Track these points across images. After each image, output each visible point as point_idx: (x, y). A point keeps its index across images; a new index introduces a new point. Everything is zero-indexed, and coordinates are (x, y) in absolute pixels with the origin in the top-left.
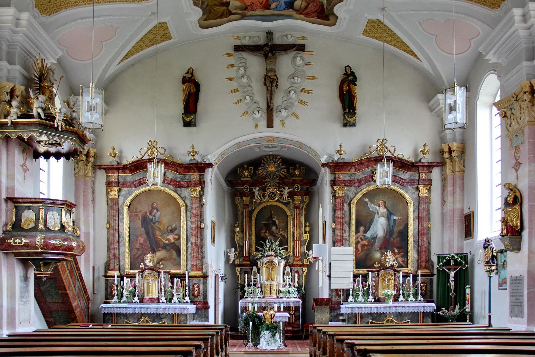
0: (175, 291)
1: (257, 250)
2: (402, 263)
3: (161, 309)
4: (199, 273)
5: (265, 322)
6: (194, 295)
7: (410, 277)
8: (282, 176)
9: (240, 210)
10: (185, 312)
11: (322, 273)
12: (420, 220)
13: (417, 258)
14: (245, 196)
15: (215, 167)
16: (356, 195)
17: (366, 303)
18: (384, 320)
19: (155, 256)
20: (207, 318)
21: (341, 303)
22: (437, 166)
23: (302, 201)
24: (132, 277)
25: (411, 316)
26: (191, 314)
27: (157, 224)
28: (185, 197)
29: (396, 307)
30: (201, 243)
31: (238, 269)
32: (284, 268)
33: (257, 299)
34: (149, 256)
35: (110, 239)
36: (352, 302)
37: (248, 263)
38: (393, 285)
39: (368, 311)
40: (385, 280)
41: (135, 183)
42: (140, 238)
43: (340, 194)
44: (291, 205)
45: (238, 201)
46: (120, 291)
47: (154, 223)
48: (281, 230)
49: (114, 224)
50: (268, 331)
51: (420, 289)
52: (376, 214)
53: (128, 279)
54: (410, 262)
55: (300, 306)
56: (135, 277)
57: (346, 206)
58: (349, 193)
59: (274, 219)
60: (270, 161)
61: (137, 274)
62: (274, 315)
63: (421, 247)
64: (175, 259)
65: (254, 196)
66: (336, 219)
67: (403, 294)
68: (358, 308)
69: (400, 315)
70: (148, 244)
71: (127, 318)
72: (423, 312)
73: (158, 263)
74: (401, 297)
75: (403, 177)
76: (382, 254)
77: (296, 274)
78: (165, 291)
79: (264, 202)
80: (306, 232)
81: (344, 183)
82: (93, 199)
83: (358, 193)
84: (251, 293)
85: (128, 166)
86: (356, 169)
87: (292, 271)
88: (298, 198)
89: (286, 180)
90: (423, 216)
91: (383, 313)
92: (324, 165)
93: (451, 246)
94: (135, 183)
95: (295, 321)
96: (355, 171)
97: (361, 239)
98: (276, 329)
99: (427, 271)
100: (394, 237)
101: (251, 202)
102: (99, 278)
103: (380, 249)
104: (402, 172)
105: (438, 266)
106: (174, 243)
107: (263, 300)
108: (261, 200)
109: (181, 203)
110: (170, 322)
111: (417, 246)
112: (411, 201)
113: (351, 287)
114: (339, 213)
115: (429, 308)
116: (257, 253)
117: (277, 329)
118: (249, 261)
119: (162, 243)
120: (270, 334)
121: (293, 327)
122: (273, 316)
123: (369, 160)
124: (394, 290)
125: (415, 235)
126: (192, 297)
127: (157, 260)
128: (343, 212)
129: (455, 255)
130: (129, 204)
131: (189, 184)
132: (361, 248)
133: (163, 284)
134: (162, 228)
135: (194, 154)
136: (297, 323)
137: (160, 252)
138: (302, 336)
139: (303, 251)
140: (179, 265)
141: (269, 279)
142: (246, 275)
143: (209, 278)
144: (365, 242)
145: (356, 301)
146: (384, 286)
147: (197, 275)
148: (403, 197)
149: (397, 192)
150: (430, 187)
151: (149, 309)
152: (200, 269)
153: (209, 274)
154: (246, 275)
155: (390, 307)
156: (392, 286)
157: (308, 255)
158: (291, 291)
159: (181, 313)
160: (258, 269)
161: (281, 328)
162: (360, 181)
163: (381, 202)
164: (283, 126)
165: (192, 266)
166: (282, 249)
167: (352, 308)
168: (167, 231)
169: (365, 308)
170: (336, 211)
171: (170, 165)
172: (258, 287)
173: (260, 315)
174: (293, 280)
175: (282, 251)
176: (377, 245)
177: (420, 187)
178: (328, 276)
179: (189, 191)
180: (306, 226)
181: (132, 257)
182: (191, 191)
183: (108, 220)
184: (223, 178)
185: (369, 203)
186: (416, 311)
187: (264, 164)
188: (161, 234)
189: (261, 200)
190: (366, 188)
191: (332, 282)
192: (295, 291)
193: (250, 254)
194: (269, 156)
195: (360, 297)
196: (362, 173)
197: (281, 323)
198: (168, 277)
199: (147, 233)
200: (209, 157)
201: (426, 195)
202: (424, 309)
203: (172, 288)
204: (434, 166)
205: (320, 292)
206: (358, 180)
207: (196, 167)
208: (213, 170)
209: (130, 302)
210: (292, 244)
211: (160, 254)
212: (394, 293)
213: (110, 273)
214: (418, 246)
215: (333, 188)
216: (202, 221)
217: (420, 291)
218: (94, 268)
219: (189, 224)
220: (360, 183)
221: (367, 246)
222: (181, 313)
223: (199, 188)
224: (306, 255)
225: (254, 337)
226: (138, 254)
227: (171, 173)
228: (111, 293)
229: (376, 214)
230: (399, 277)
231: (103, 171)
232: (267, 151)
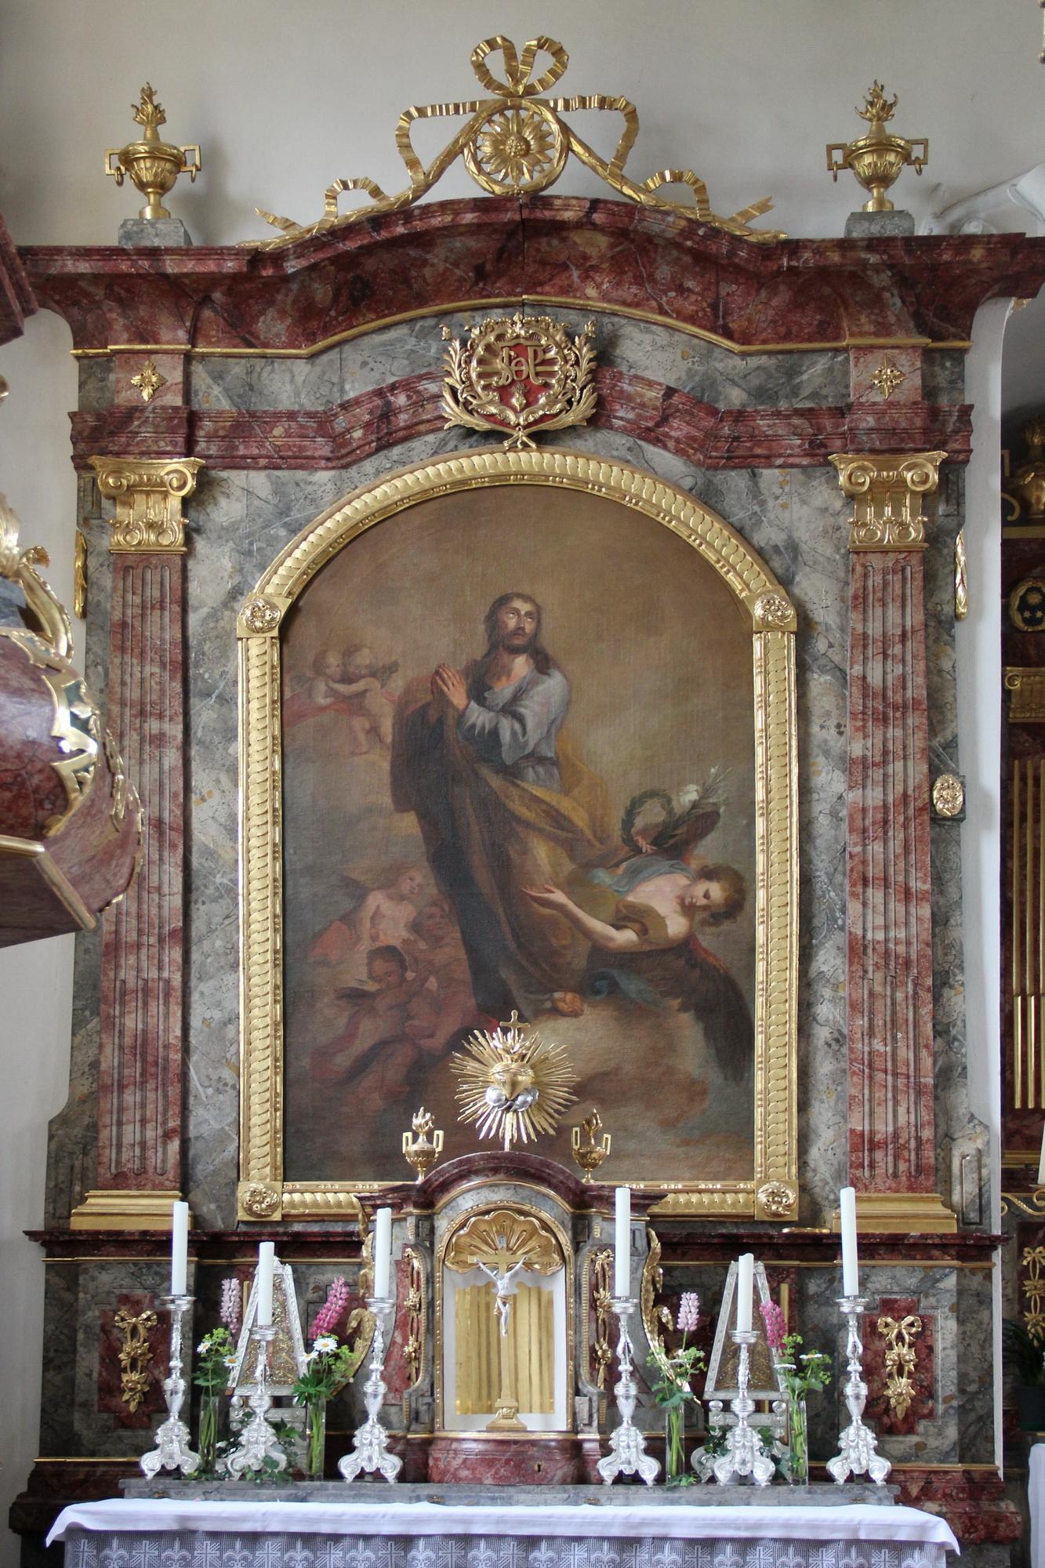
27: (535, 783)
42: (376, 900)
47: (511, 773)
64: (695, 1090)
70: (452, 951)
106: (686, 947)
119: (584, 947)
134: (580, 819)
137: (563, 1024)
165: (856, 1148)
168: (629, 840)
188: (568, 867)
227: (662, 337)
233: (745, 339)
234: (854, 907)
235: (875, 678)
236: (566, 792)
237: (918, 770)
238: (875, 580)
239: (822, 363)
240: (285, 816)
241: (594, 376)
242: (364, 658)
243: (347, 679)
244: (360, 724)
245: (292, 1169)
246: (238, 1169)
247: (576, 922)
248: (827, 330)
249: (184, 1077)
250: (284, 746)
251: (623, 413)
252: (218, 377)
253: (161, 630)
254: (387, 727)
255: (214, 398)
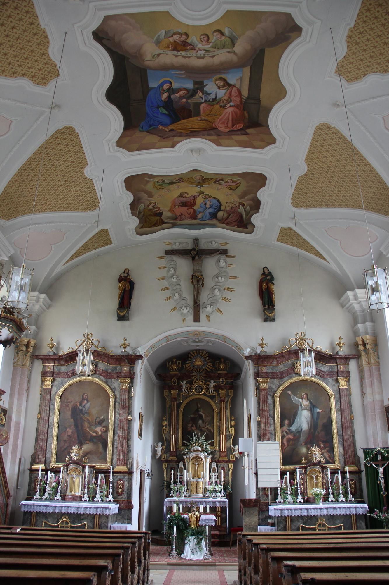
0: (98, 488)
1: (184, 445)
2: (328, 458)
3: (82, 509)
4: (124, 469)
5: (190, 525)
6: (117, 492)
7: (338, 473)
8: (208, 370)
9: (168, 403)
10: (107, 512)
11: (249, 470)
12: (343, 412)
13: (343, 453)
14: (173, 389)
15: (145, 360)
16: (279, 387)
17: (295, 504)
18: (315, 525)
19: (81, 449)
20: (129, 521)
21: (270, 504)
22: (354, 358)
23: (227, 395)
24: (57, 471)
25: (343, 519)
26: (113, 515)
27: (86, 416)
28: (115, 388)
29: (327, 508)
30: (127, 436)
31: (165, 465)
32: (211, 464)
33: (183, 498)
34: (75, 448)
35: (40, 430)
36: (280, 502)
37: (175, 458)
38: (321, 483)
39: (298, 513)
40: (313, 478)
41: (68, 373)
42: (68, 429)
43: (264, 386)
44: (217, 399)
45: (166, 394)
46: (43, 486)
47: (83, 414)
48: (207, 423)
49: (45, 414)
50: (194, 537)
51: (349, 487)
52: (300, 406)
53: (53, 474)
54: (337, 458)
55: (227, 506)
56: (60, 471)
57: (270, 398)
58: (272, 385)
59: (200, 413)
60: (197, 355)
61: (62, 468)
62: (200, 518)
63: (347, 441)
64: (101, 453)
65: (182, 389)
66: (261, 412)
67: (333, 494)
68: (288, 510)
69: (332, 518)
70: (76, 436)
71: (46, 518)
72: (356, 514)
73: (84, 457)
74: (331, 496)
75: (323, 370)
76: (308, 449)
77: (222, 471)
78: (88, 488)
79: (191, 395)
80: (231, 427)
81: (267, 375)
82: (28, 388)
83: (281, 385)
84: (177, 492)
85: (63, 357)
86: (277, 361)
87: (219, 467)
88: (223, 392)
89: (212, 374)
90: (345, 409)
91: (314, 515)
92: (247, 358)
93: (375, 440)
94: (68, 373)
95: (222, 523)
96: (277, 364)
97: (286, 432)
98: (201, 535)
99: (354, 467)
100: (319, 430)
101: (179, 395)
102: (24, 471)
103: (306, 443)
104: (321, 365)
105: (365, 462)
106: (101, 435)
107: (189, 500)
108: (189, 393)
109: (111, 394)
110: (91, 525)
111: (342, 440)
112: (333, 393)
113: (278, 485)
114: (263, 406)
115: (361, 509)
116: (183, 448)
117: (203, 535)
118: (176, 456)
120: (195, 540)
121: (220, 531)
122: (198, 519)
123: (289, 352)
124: (323, 489)
125: (339, 428)
126: (115, 495)
127: (83, 454)
128: (268, 405)
129: (381, 449)
130: (61, 394)
131: (119, 375)
132: (287, 443)
133: (86, 480)
134: (90, 420)
135: (125, 346)
136: (224, 526)
137: (87, 445)
138: (229, 542)
139: (229, 446)
140: (104, 460)
141: (195, 476)
142: (173, 471)
143: (134, 474)
144: (291, 436)
145: (284, 502)
146: (312, 484)
147: (122, 471)
148: (325, 389)
149: (318, 384)
150: (349, 379)
151: (70, 508)
152: (126, 464)
153: (135, 470)
154: (173, 471)
155: (321, 509)
156: (320, 484)
157: (234, 450)
158: (217, 489)
159: (103, 514)
160: (185, 465)
161: (207, 534)
162: (282, 373)
163: (303, 394)
164: (209, 320)
166: (209, 444)
167: (281, 510)
168: (95, 423)
169: (295, 509)
170: (261, 404)
171: (103, 357)
172: (184, 485)
173: (185, 517)
174: (219, 477)
175: (208, 446)
176: (302, 439)
177: (340, 379)
178: (254, 473)
179: (118, 382)
180: (231, 420)
181: (59, 449)
182: (121, 383)
183: (39, 410)
184: (153, 370)
185: (292, 396)
186: (348, 513)
187: (191, 358)
188: (89, 426)
189: (189, 393)
190: (288, 380)
191: (259, 479)
192: (221, 490)
193: (177, 449)
194: (196, 350)
195: (289, 497)
196: (284, 366)
197: (207, 527)
198: (92, 472)
199: (76, 425)
200: (139, 349)
201: (346, 387)
202: (356, 511)
203: (95, 485)
204: (350, 358)
205: (247, 490)
206: (280, 373)
207: (126, 359)
208: (143, 362)
209: (51, 499)
210: (218, 438)
211: (87, 447)
212: (324, 492)
213: (36, 466)
214: (343, 440)
215: (257, 381)
216: (130, 413)
217: (349, 490)
218: (20, 460)
219: (117, 416)
220: (282, 376)
221: (292, 440)
222: (103, 514)
223: (128, 380)
224: (232, 450)
225: (179, 544)
226: (65, 447)
228: (35, 488)
229: (300, 406)
230: (327, 474)
231: (41, 361)
232: (194, 346)
233: (111, 364)
234: (119, 431)
235: (123, 404)
236: (89, 417)
237: (127, 415)
238: (123, 392)
239: (119, 367)
240: (59, 419)
241: (95, 368)
242: (69, 400)
243: (67, 403)
244: (68, 408)
245: (57, 462)
246: (51, 462)
247: (89, 433)
248: (119, 364)
249: (46, 450)
250: (60, 410)
251: (98, 372)
252: (57, 368)
253: (48, 397)
254: (71, 409)
255: (56, 370)
